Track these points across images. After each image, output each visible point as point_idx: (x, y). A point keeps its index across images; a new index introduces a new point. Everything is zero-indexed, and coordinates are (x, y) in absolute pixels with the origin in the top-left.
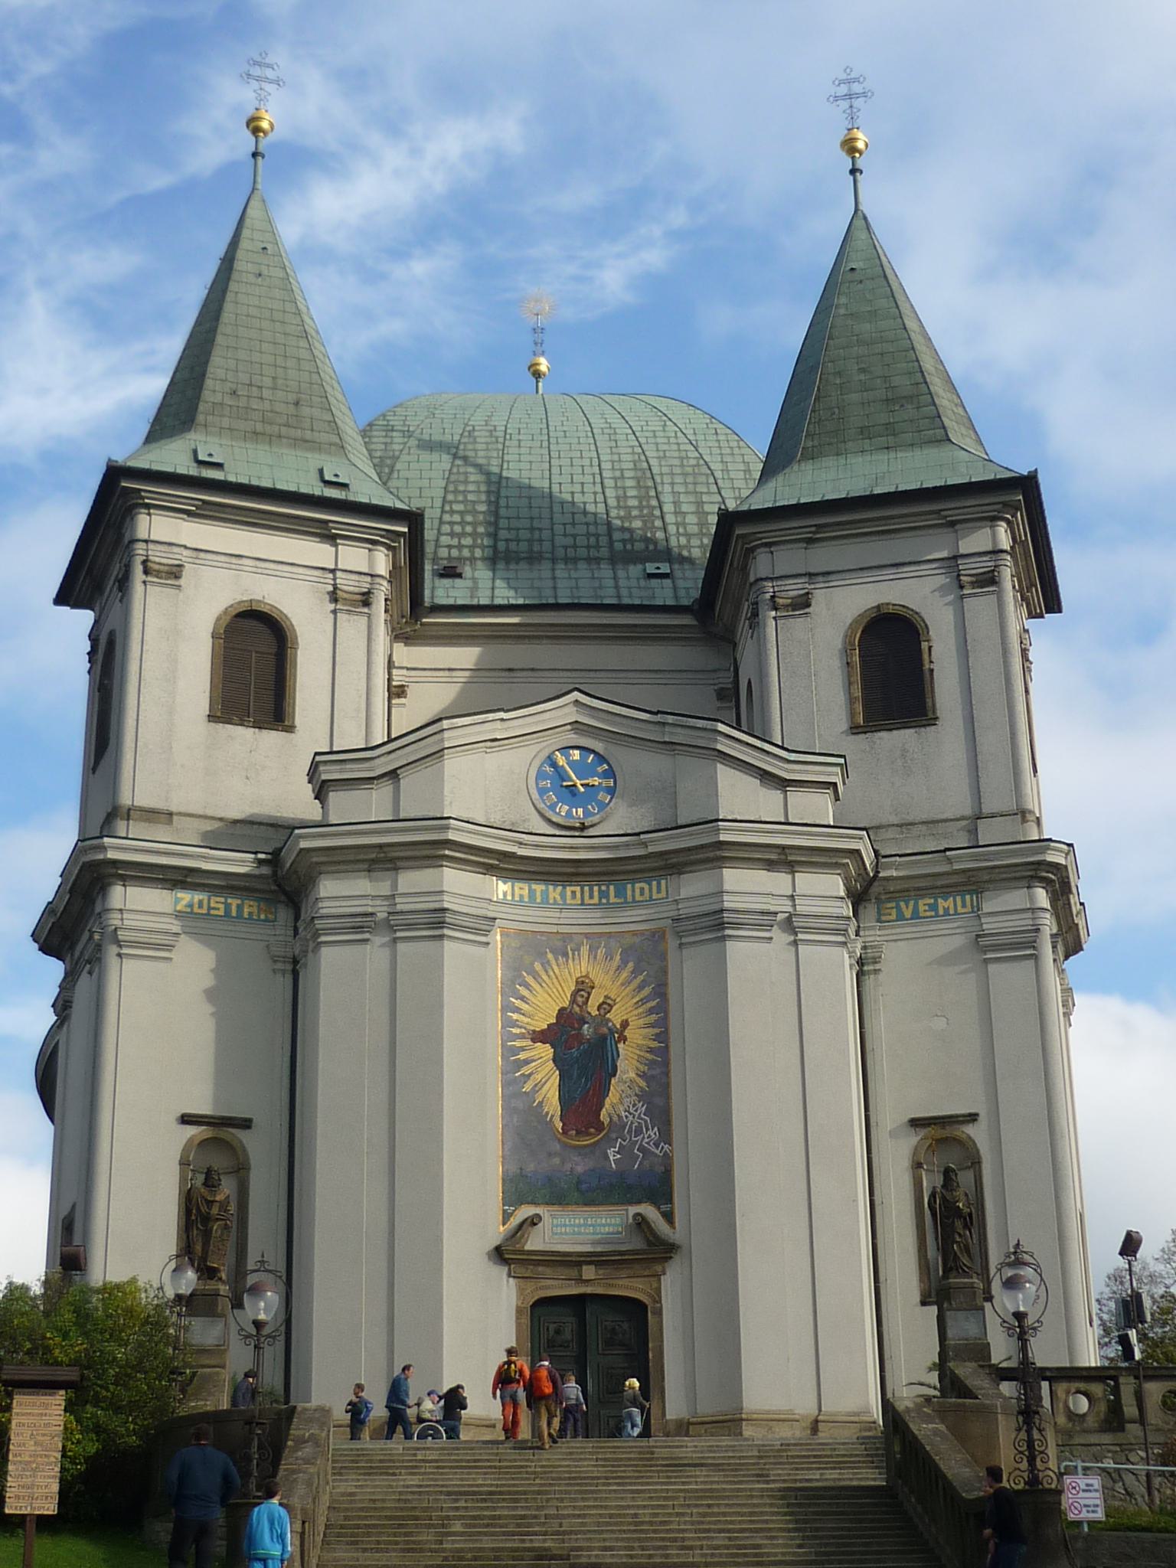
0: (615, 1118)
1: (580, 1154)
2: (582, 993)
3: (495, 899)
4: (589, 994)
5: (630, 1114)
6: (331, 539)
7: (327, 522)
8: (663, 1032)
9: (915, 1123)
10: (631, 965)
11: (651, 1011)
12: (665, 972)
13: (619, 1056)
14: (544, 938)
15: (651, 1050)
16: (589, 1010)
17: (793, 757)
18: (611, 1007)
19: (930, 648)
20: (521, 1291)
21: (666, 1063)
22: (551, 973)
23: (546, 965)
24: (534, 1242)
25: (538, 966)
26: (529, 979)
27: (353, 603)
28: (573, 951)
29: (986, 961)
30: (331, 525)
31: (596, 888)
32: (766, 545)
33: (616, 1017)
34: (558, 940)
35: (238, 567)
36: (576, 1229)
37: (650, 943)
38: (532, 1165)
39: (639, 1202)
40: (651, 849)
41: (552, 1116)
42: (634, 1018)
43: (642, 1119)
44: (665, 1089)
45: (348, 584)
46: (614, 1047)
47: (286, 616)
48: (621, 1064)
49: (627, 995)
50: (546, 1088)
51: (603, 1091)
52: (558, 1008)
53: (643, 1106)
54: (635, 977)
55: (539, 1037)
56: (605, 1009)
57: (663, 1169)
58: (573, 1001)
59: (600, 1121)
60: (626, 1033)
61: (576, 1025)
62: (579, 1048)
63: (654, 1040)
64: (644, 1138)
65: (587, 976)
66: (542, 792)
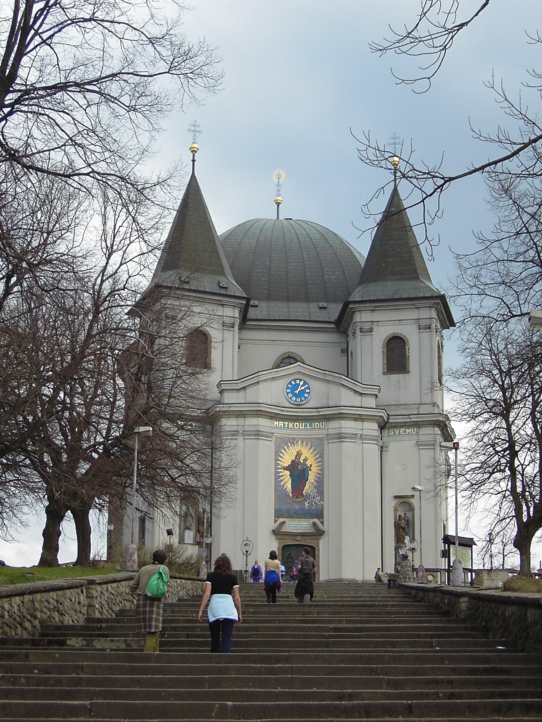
9: (396, 497)
10: (313, 448)
11: (319, 462)
15: (319, 474)
17: (364, 386)
20: (279, 543)
21: (323, 478)
23: (288, 447)
24: (283, 530)
25: (286, 447)
26: (283, 451)
27: (228, 327)
29: (419, 449)
32: (360, 311)
39: (314, 518)
40: (320, 413)
45: (227, 320)
55: (285, 468)
58: (296, 458)
66: (288, 393)
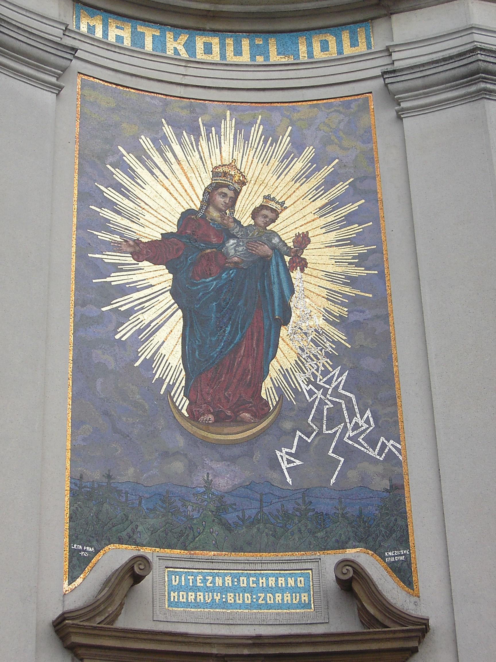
0: (290, 396)
1: (223, 458)
2: (225, 190)
3: (74, 28)
4: (237, 193)
5: (318, 387)
8: (371, 252)
10: (309, 152)
12: (372, 160)
13: (292, 292)
14: (156, 102)
16: (237, 216)
18: (277, 214)
22: (170, 155)
25: (146, 142)
26: (130, 159)
28: (208, 127)
31: (245, 43)
34: (182, 108)
36: (217, 598)
37: (342, 117)
39: (342, 545)
41: (170, 387)
43: (340, 396)
46: (283, 275)
49: (304, 196)
53: (340, 374)
54: (318, 169)
56: (266, 217)
57: (386, 484)
60: (306, 254)
61: (214, 240)
62: (219, 277)
63: (357, 265)
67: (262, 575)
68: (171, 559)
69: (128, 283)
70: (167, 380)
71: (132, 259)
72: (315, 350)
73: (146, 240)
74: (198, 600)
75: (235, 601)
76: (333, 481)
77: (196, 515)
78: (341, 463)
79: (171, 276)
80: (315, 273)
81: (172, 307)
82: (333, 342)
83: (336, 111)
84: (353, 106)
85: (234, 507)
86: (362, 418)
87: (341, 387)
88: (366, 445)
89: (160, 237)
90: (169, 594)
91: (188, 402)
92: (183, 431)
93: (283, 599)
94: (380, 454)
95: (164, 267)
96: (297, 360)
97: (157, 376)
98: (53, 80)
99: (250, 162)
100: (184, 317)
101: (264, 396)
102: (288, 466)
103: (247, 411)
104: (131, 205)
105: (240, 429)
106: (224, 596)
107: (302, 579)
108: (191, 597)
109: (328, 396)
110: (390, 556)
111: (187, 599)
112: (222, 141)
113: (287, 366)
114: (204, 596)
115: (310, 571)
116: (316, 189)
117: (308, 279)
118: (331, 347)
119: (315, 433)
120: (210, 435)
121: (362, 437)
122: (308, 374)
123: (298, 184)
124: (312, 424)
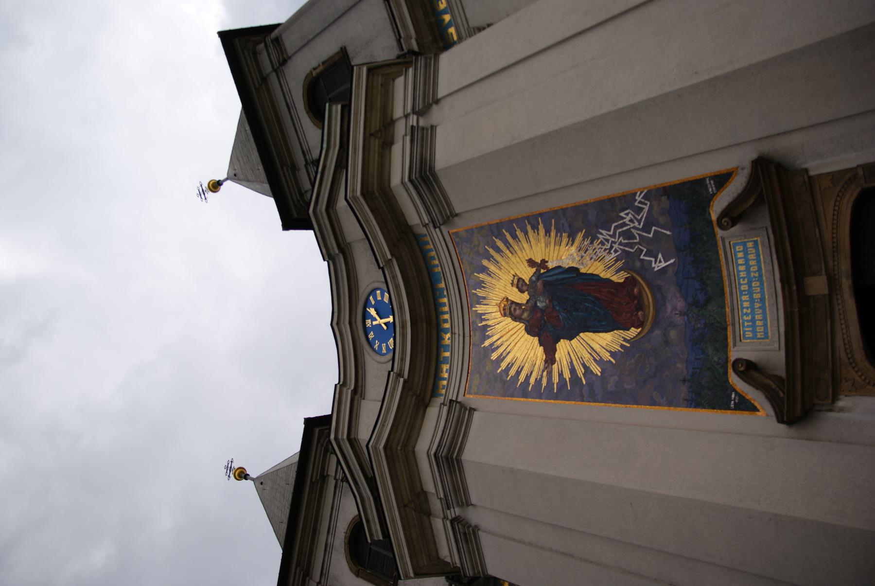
0: (619, 264)
2: (512, 309)
4: (513, 302)
5: (612, 247)
6: (324, 478)
7: (312, 483)
8: (529, 223)
10: (485, 263)
11: (515, 237)
12: (481, 228)
15: (548, 232)
16: (525, 302)
17: (325, 146)
18: (520, 279)
19: (315, 69)
21: (554, 213)
22: (499, 342)
25: (494, 356)
26: (503, 365)
28: (482, 320)
30: (314, 480)
33: (527, 273)
34: (475, 335)
35: (331, 546)
38: (679, 365)
41: (625, 340)
42: (524, 254)
43: (615, 233)
44: (580, 210)
47: (353, 519)
48: (567, 263)
49: (507, 263)
50: (597, 347)
51: (593, 278)
52: (527, 336)
53: (601, 234)
54: (492, 257)
56: (522, 285)
57: (664, 198)
59: (624, 281)
60: (538, 260)
63: (538, 230)
64: (634, 228)
65: (499, 305)
67: (738, 275)
68: (734, 338)
69: (569, 367)
70: (621, 342)
71: (555, 365)
72: (590, 251)
73: (544, 355)
74: (761, 318)
75: (758, 293)
76: (668, 233)
77: (703, 321)
78: (656, 228)
79: (562, 340)
80: (547, 254)
81: (579, 339)
82: (584, 240)
83: (462, 250)
84: (457, 240)
85: (694, 296)
86: (625, 218)
87: (609, 233)
88: (642, 214)
89: (541, 347)
90: (759, 339)
91: (632, 328)
92: (651, 331)
93: (754, 260)
94: (646, 204)
95: (557, 345)
96: (598, 261)
97: (620, 349)
98: (467, 412)
99: (496, 296)
100: (583, 332)
101: (622, 280)
102: (663, 262)
103: (633, 290)
104: (527, 364)
105: (644, 293)
106: (756, 300)
107: (737, 247)
108: (759, 323)
109: (616, 240)
110: (712, 190)
111: (761, 326)
112: (488, 312)
113: (602, 267)
114: (758, 314)
115: (731, 243)
116: (503, 257)
117: (551, 258)
118: (587, 241)
119: (640, 247)
120: (651, 314)
121: (637, 216)
122: (605, 254)
123: (502, 267)
124: (635, 249)
